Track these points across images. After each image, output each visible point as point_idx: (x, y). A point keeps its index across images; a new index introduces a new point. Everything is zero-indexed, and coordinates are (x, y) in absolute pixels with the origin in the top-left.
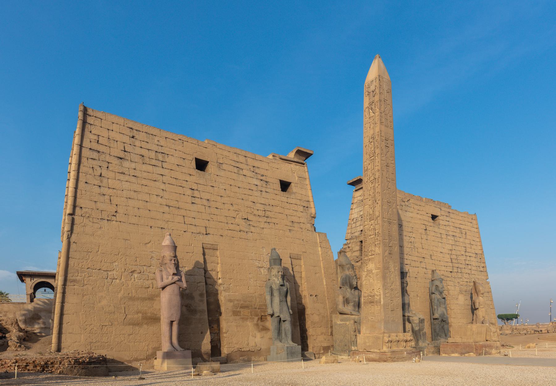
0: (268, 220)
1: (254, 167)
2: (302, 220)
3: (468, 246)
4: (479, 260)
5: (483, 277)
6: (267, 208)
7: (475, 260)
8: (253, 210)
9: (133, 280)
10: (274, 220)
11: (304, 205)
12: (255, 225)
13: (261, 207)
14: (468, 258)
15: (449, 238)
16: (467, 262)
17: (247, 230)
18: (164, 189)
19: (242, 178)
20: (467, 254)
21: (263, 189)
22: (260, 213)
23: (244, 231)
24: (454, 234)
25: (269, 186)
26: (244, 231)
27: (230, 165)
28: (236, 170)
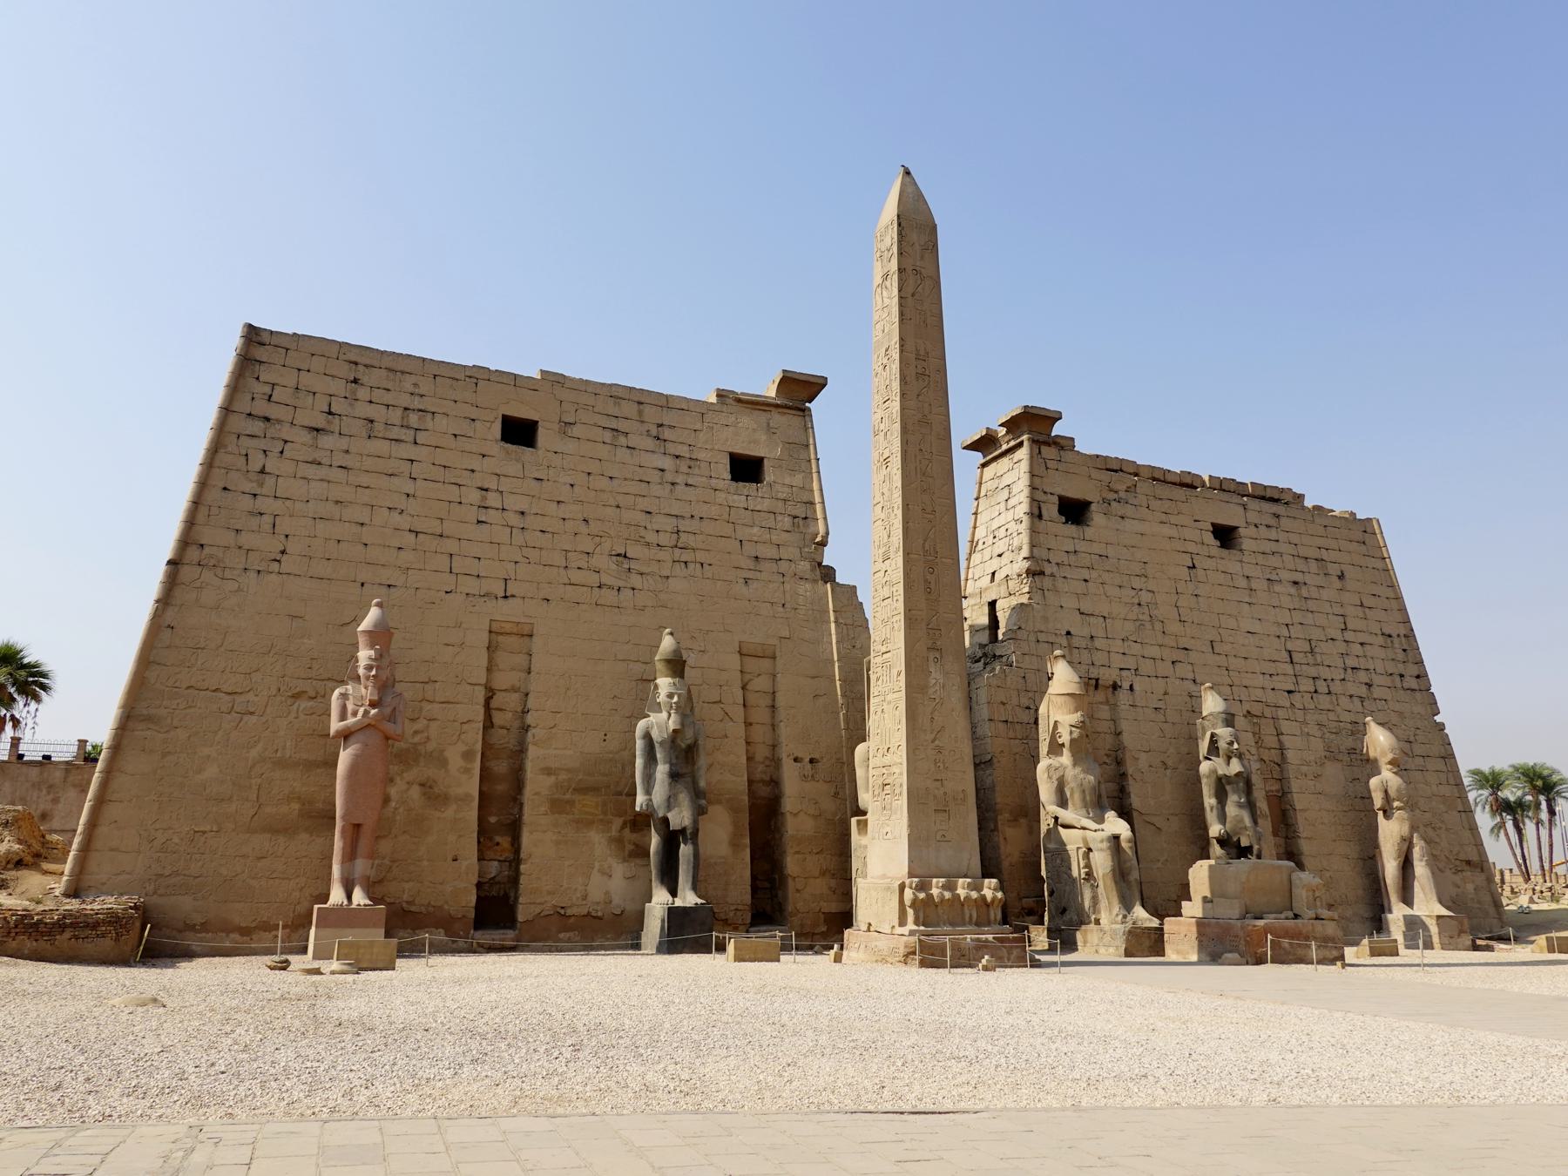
0: (686, 556)
1: (661, 425)
2: (784, 554)
3: (1350, 611)
4: (1401, 656)
5: (1418, 709)
6: (685, 525)
7: (1381, 653)
8: (643, 532)
9: (293, 715)
10: (700, 556)
11: (794, 513)
12: (644, 569)
13: (668, 525)
14: (1357, 649)
15: (1277, 588)
16: (1351, 662)
17: (621, 584)
18: (411, 492)
19: (623, 454)
20: (1349, 636)
21: (680, 479)
22: (665, 539)
23: (611, 587)
24: (1298, 577)
25: (696, 471)
26: (611, 587)
27: (595, 425)
28: (608, 436)
